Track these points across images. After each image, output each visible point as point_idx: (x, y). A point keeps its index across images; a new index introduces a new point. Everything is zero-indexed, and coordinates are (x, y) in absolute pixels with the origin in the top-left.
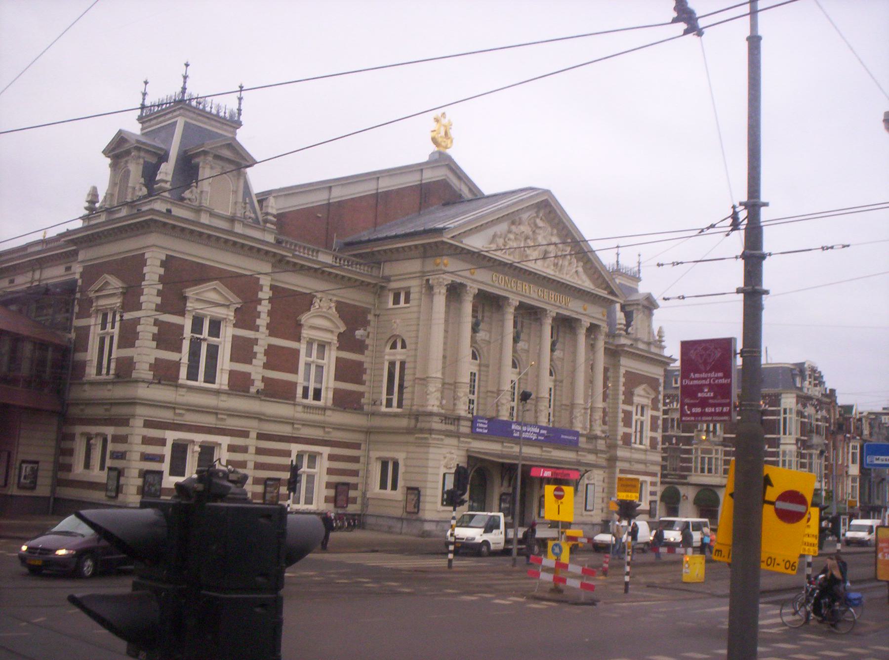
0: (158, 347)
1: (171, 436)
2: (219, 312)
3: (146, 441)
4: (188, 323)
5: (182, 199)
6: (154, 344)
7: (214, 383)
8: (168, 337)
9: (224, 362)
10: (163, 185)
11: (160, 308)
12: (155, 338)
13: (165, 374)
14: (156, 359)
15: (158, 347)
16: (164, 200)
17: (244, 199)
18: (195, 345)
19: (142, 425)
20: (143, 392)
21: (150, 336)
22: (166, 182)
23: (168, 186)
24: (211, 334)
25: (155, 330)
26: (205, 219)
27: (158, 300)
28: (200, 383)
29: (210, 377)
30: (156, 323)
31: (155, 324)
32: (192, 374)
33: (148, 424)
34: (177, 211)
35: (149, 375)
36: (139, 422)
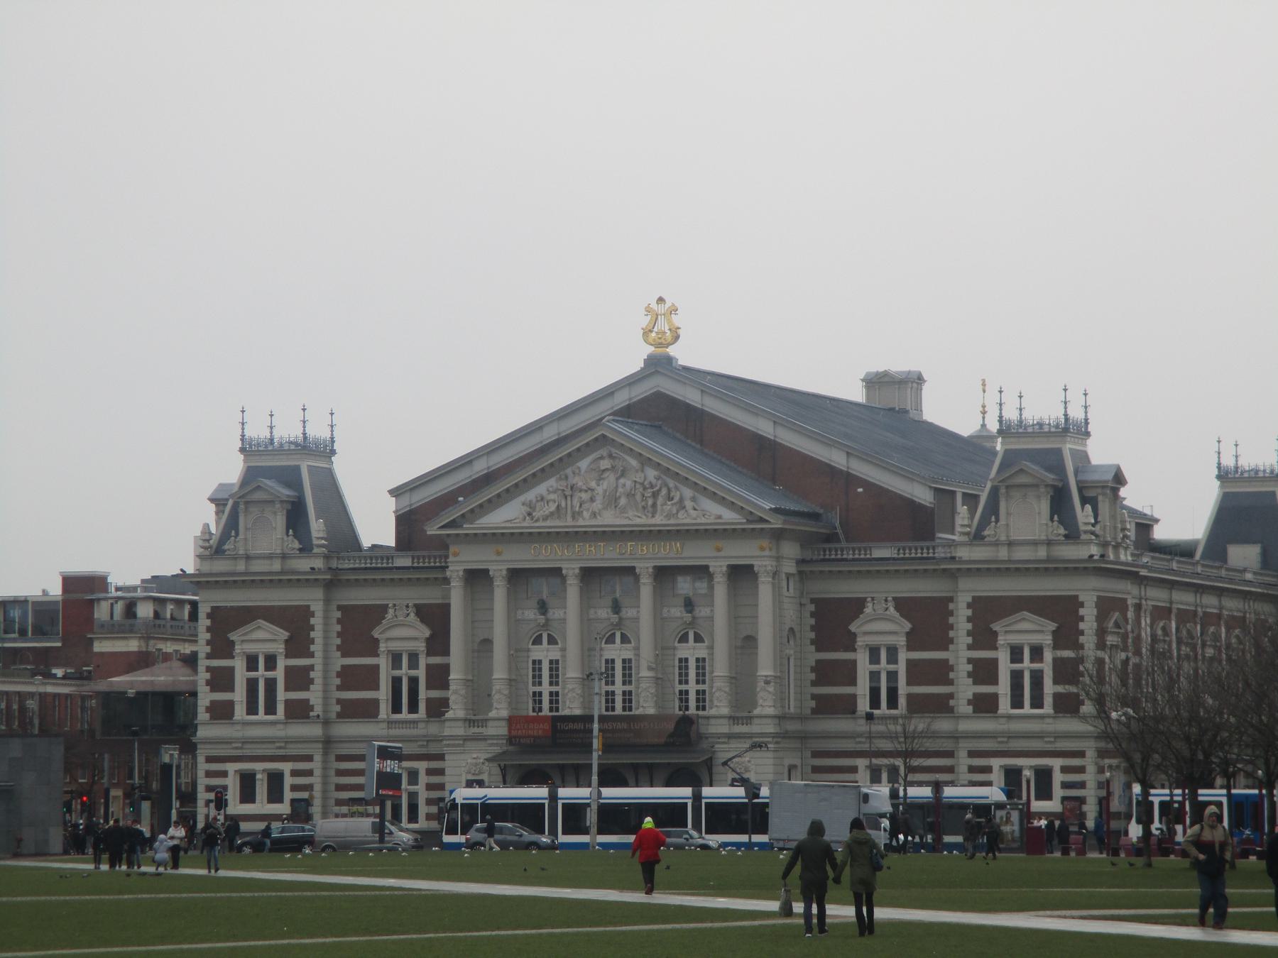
0: (975, 683)
1: (996, 763)
2: (1036, 639)
4: (1003, 657)
5: (983, 538)
7: (1041, 706)
8: (984, 671)
9: (1049, 688)
11: (970, 647)
12: (969, 675)
13: (985, 705)
14: (974, 694)
15: (975, 683)
17: (1052, 519)
18: (1017, 677)
20: (964, 726)
21: (965, 674)
24: (1032, 661)
25: (970, 668)
26: (1003, 553)
27: (970, 640)
28: (1027, 710)
29: (1037, 702)
30: (970, 661)
32: (1017, 702)
33: (972, 754)
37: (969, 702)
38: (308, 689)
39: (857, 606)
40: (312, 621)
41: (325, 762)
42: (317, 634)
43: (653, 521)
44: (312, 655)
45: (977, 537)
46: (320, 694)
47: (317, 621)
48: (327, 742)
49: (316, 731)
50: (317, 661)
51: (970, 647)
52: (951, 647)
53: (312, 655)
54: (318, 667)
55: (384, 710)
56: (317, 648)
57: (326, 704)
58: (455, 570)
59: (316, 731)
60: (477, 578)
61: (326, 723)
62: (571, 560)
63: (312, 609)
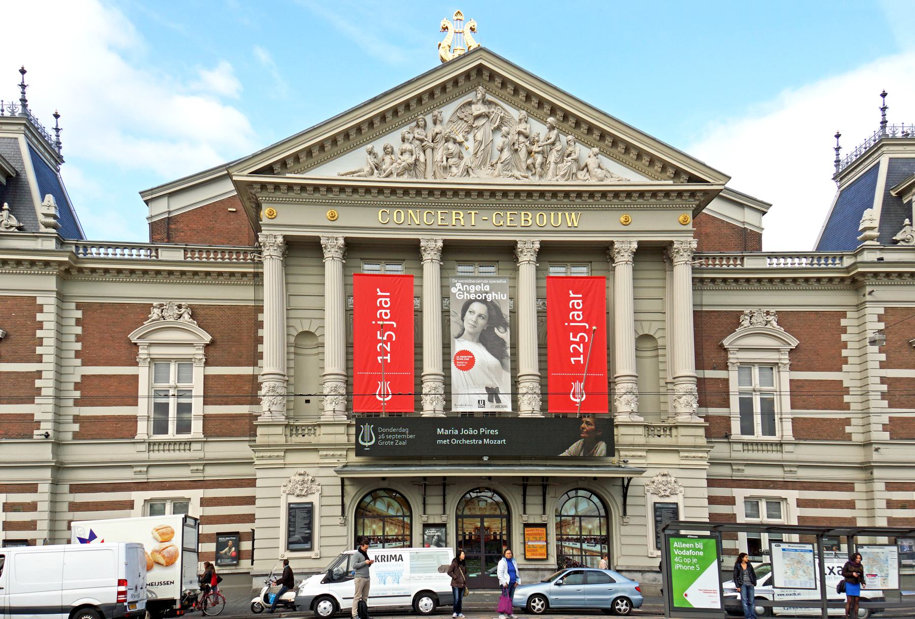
3: (890, 504)
6: (885, 403)
10: (868, 233)
12: (884, 396)
15: (890, 406)
16: (872, 249)
19: (884, 488)
22: (872, 229)
23: (875, 233)
25: (885, 388)
31: (882, 383)
33: (891, 486)
34: (889, 257)
35: (886, 436)
36: (882, 486)
37: (885, 428)
38: (33, 402)
39: (732, 320)
40: (39, 317)
41: (54, 493)
42: (48, 334)
43: (543, 181)
44: (39, 359)
45: (888, 241)
46: (50, 408)
47: (48, 317)
48: (59, 468)
49: (45, 453)
50: (48, 367)
51: (883, 365)
52: (845, 367)
53: (39, 359)
54: (49, 375)
55: (143, 429)
56: (47, 350)
57: (57, 421)
58: (271, 240)
59: (45, 453)
60: (301, 249)
61: (58, 445)
62: (430, 226)
63: (39, 301)
